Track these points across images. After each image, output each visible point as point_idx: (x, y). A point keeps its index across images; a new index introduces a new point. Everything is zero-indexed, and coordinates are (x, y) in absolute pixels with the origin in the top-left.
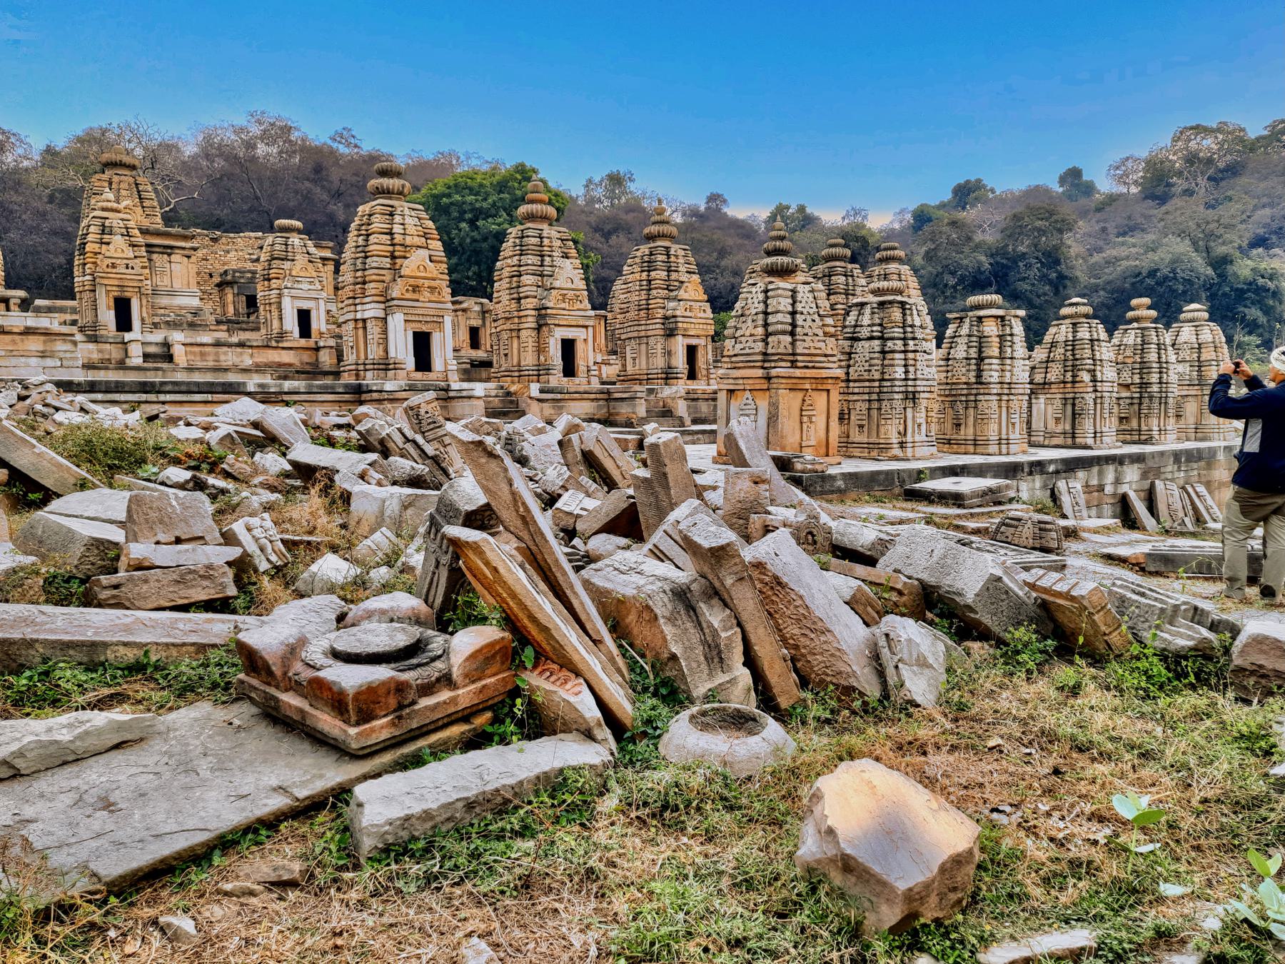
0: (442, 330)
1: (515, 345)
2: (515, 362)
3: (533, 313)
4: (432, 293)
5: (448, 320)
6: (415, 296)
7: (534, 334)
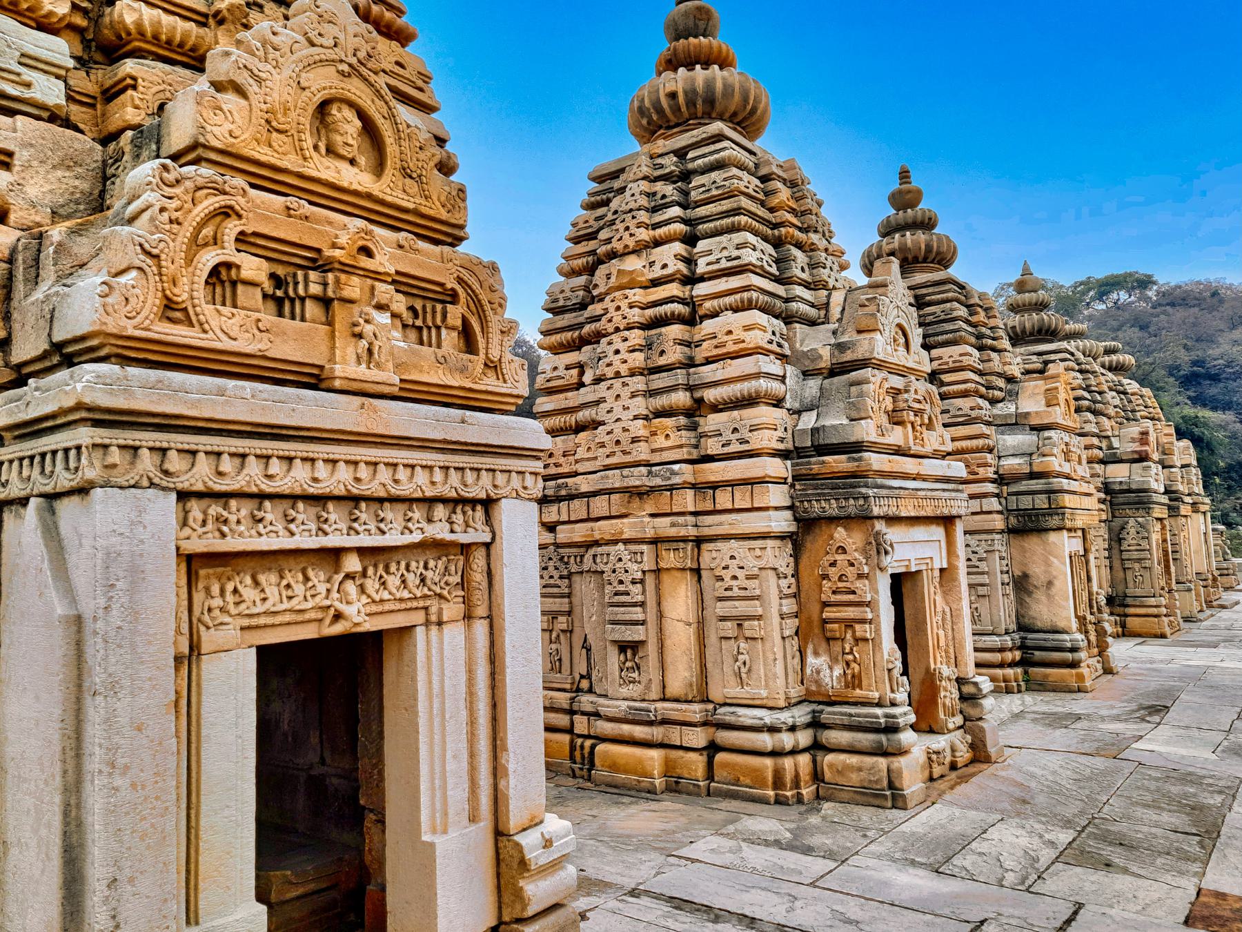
0: (481, 607)
1: (680, 601)
2: (681, 676)
3: (777, 468)
4: (419, 327)
5: (519, 530)
6: (293, 341)
7: (778, 556)
